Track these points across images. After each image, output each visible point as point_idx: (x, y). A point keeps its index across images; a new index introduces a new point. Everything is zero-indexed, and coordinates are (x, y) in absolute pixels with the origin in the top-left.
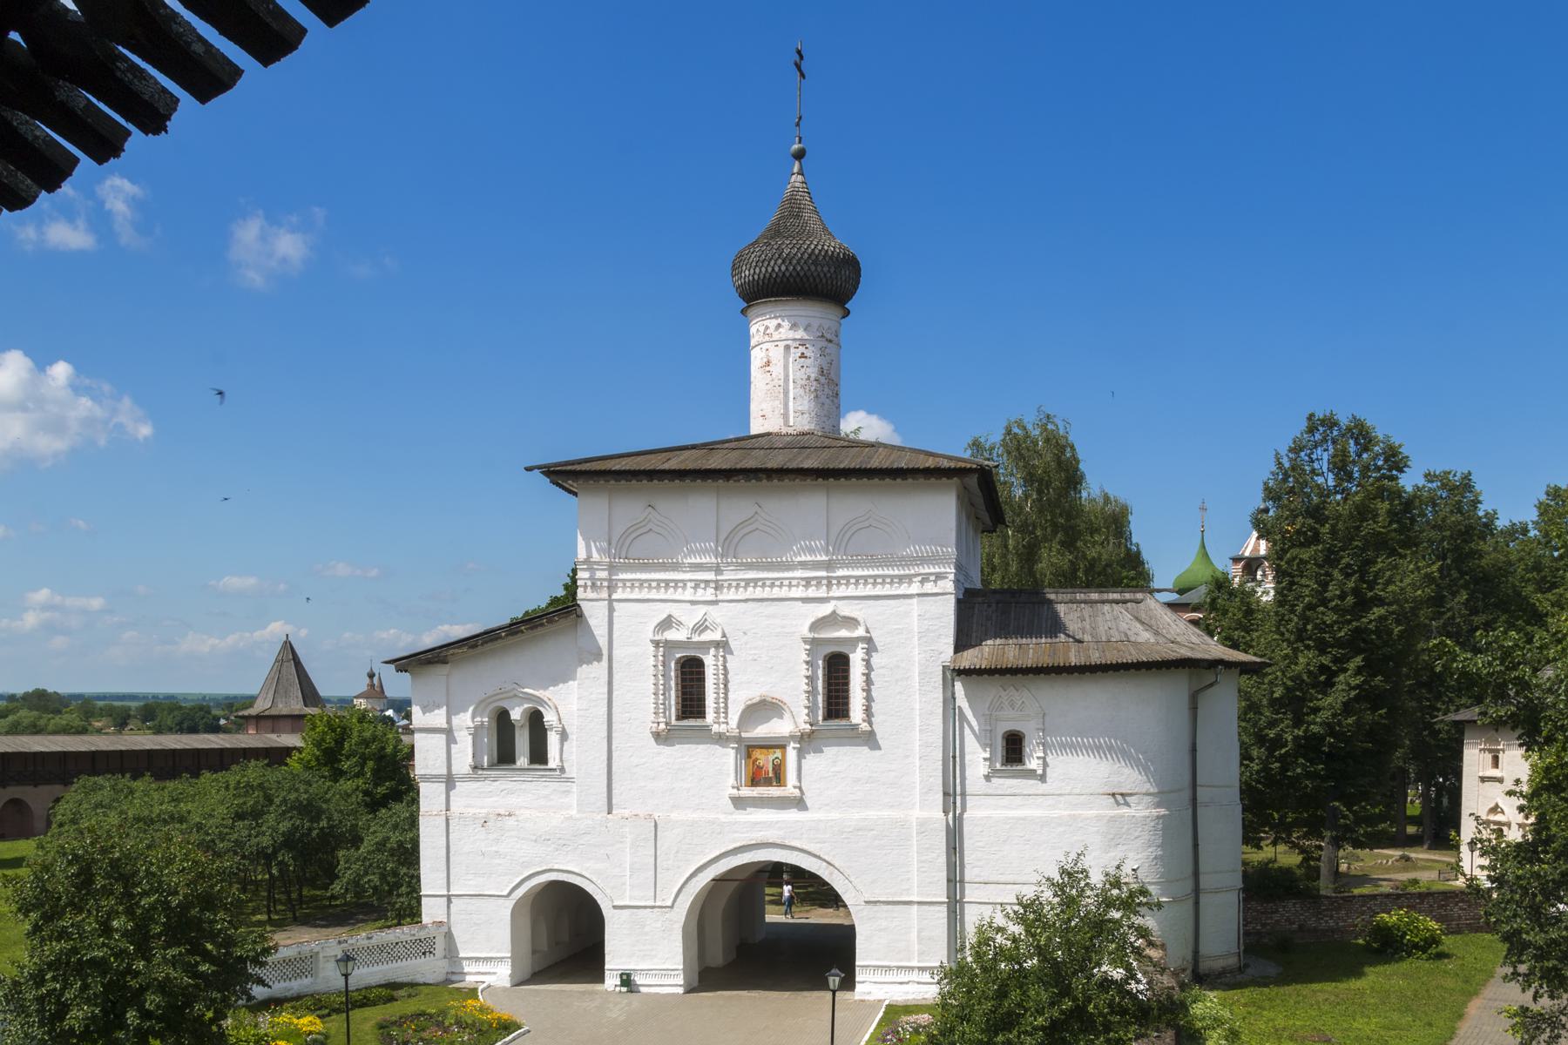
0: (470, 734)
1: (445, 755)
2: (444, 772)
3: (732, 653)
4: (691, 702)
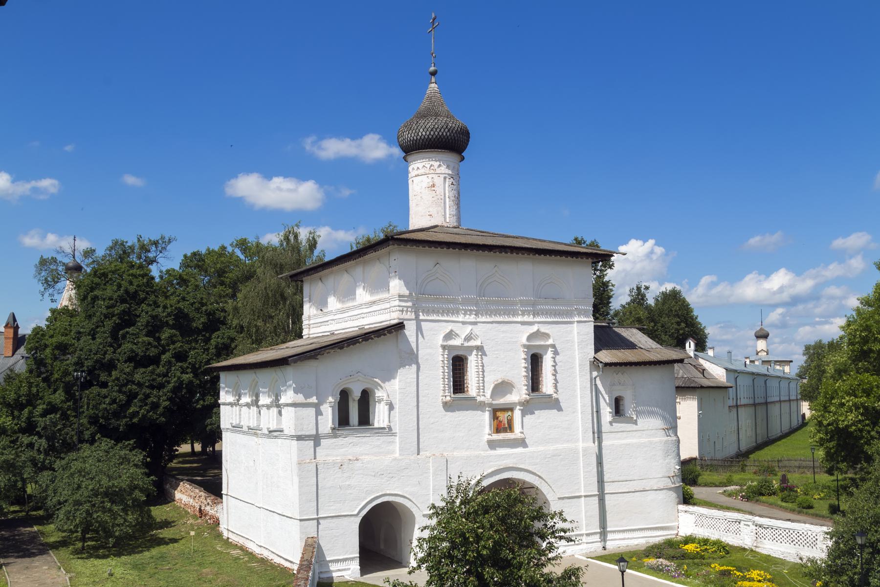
0: (330, 407)
1: (315, 422)
2: (314, 432)
3: (486, 355)
4: (458, 384)
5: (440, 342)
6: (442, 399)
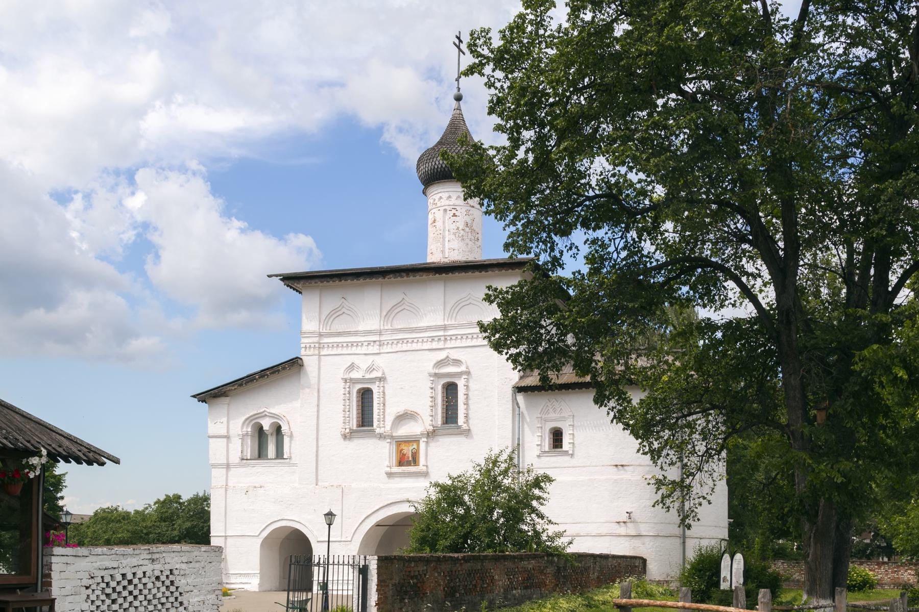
4: (365, 418)
5: (341, 374)
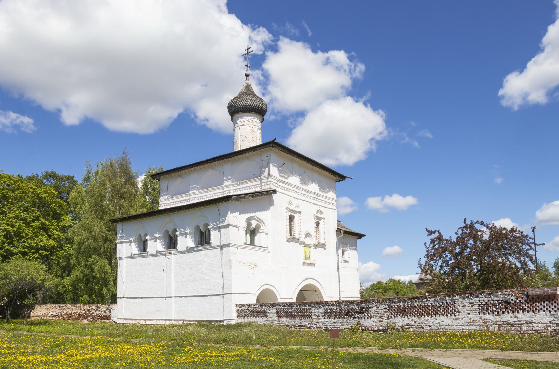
6: (287, 237)
